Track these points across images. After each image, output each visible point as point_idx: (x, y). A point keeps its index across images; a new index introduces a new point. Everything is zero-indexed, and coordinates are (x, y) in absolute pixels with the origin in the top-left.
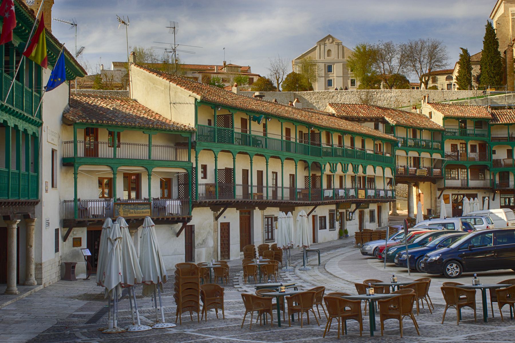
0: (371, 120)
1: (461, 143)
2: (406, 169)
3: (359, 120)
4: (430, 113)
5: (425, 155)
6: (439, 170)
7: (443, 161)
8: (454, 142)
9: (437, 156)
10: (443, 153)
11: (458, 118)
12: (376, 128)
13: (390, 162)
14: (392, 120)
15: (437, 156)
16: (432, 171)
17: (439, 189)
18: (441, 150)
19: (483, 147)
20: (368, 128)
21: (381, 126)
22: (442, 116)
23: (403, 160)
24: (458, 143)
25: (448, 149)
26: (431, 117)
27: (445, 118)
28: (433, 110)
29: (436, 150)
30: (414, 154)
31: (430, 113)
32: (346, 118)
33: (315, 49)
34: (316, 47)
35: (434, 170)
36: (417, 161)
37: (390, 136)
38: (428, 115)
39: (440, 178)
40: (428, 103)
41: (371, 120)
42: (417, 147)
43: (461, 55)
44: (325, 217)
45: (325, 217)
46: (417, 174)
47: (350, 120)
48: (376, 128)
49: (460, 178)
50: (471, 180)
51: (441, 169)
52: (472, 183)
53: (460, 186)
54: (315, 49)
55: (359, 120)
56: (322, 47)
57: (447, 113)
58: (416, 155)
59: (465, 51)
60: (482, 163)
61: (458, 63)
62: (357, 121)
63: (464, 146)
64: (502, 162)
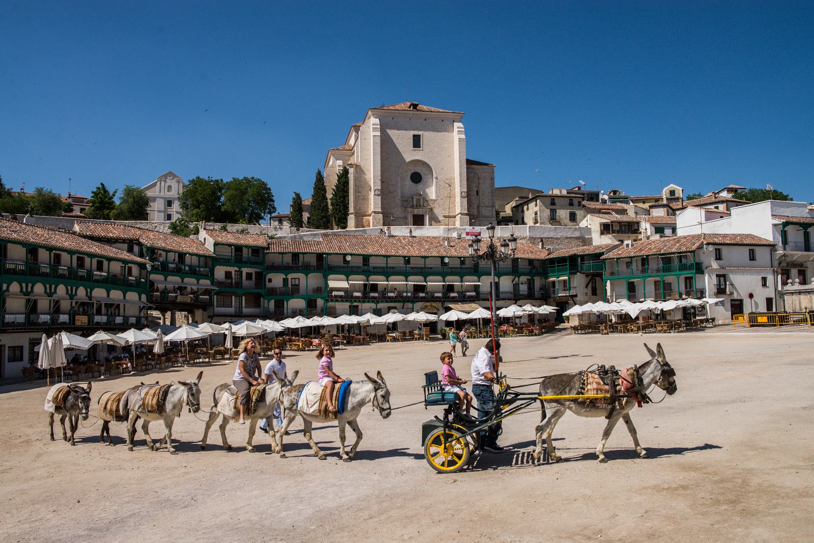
0: (124, 241)
4: (205, 239)
8: (229, 269)
10: (214, 278)
15: (205, 283)
18: (210, 275)
21: (136, 249)
28: (208, 237)
29: (205, 276)
31: (205, 239)
33: (155, 185)
34: (157, 182)
35: (201, 297)
40: (205, 229)
43: (294, 199)
44: (22, 347)
45: (22, 347)
46: (178, 300)
50: (246, 307)
53: (234, 314)
54: (155, 185)
56: (163, 183)
59: (298, 195)
61: (291, 206)
64: (278, 290)
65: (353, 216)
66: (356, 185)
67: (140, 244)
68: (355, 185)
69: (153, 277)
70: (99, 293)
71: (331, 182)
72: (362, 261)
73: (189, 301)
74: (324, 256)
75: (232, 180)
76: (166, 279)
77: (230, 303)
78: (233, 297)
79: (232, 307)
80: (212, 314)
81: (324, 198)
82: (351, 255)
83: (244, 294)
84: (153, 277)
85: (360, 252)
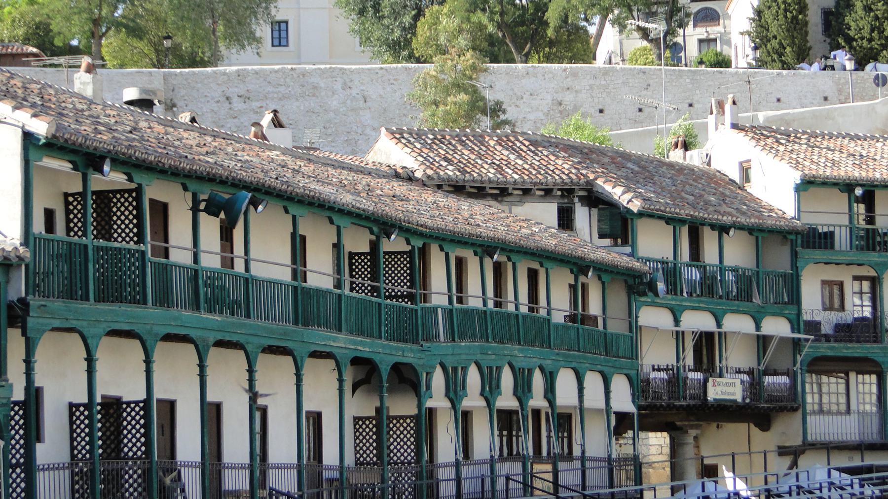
1: (856, 278)
2: (676, 380)
3: (501, 193)
5: (738, 324)
6: (784, 380)
7: (796, 344)
8: (833, 274)
9: (777, 327)
10: (799, 314)
11: (847, 187)
12: (566, 220)
14: (628, 196)
15: (777, 327)
16: (760, 383)
17: (783, 451)
20: (536, 221)
21: (582, 215)
22: (796, 177)
24: (844, 275)
26: (747, 179)
30: (698, 321)
32: (458, 189)
36: (707, 347)
37: (618, 256)
38: (734, 174)
39: (791, 403)
40: (735, 126)
42: (710, 290)
47: (470, 195)
49: (853, 406)
51: (793, 376)
55: (501, 193)
62: (495, 197)
63: (866, 285)
67: (594, 199)
73: (738, 397)
76: (677, 322)
77: (843, 400)
80: (798, 441)
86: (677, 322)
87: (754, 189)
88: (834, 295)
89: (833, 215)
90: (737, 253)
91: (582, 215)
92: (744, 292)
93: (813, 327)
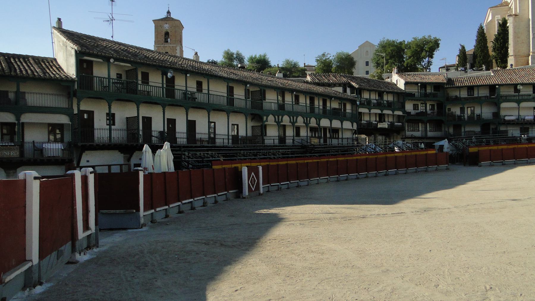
3: (329, 85)
7: (403, 117)
8: (416, 103)
9: (400, 113)
12: (345, 91)
13: (356, 117)
15: (400, 113)
19: (441, 106)
21: (348, 90)
23: (369, 116)
25: (409, 107)
27: (406, 84)
32: (318, 84)
41: (340, 85)
42: (379, 105)
48: (345, 91)
52: (430, 134)
55: (329, 85)
57: (409, 80)
58: (379, 111)
59: (463, 47)
60: (439, 118)
61: (458, 56)
65: (513, 57)
66: (515, 32)
68: (515, 32)
69: (361, 110)
70: (325, 123)
71: (492, 33)
72: (532, 89)
73: (387, 127)
74: (497, 87)
75: (413, 40)
76: (370, 111)
78: (420, 124)
79: (419, 131)
81: (486, 47)
82: (522, 84)
83: (430, 121)
84: (361, 110)
85: (531, 81)
86: (370, 111)
87: (398, 86)
88: (415, 107)
89: (414, 90)
90: (390, 98)
91: (348, 90)
92: (389, 106)
93: (409, 113)
